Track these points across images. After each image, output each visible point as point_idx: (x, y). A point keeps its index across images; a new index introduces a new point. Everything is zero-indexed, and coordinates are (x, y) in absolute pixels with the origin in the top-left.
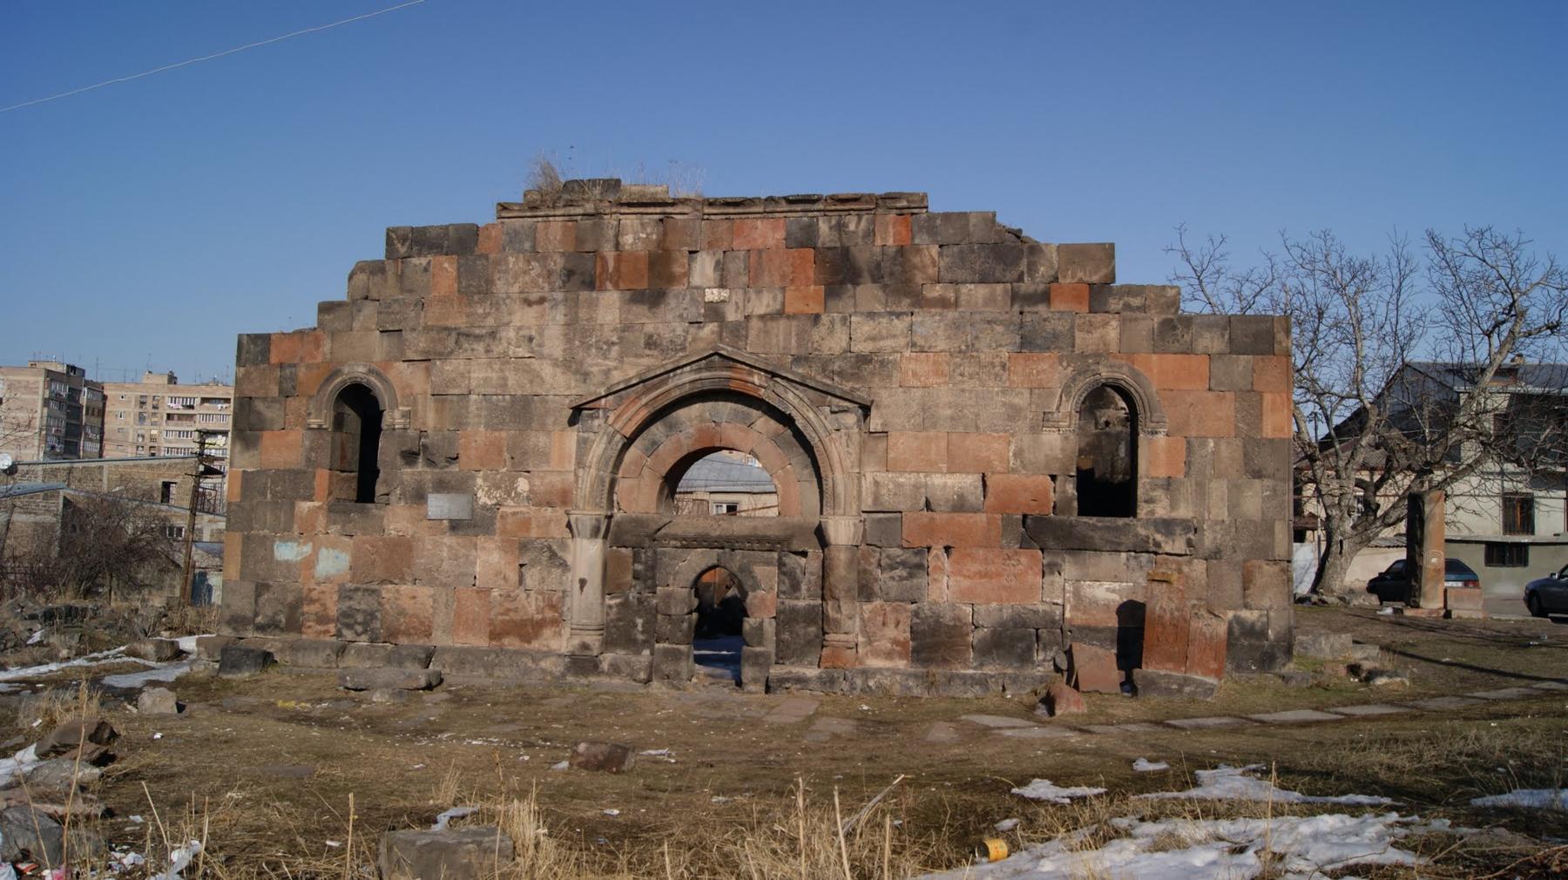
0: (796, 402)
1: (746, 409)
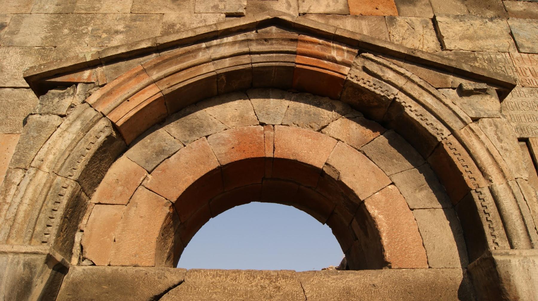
0: (401, 82)
1: (312, 109)
